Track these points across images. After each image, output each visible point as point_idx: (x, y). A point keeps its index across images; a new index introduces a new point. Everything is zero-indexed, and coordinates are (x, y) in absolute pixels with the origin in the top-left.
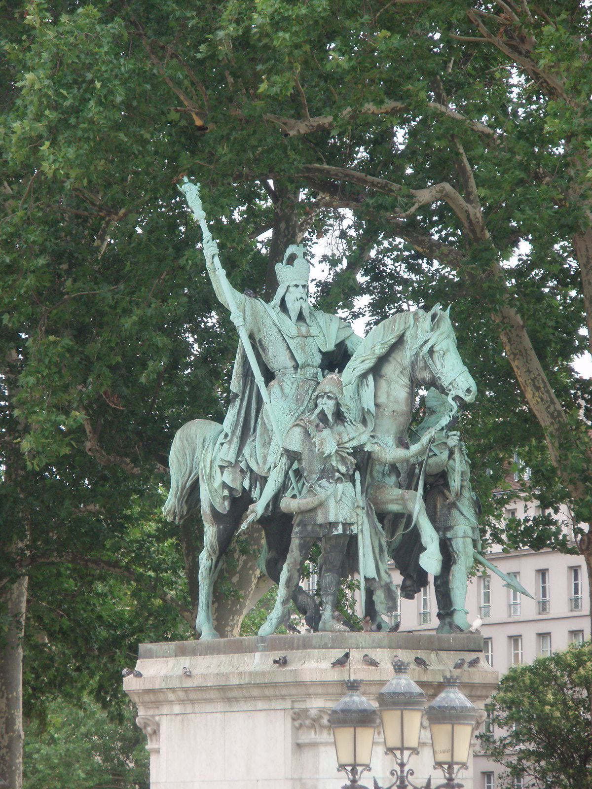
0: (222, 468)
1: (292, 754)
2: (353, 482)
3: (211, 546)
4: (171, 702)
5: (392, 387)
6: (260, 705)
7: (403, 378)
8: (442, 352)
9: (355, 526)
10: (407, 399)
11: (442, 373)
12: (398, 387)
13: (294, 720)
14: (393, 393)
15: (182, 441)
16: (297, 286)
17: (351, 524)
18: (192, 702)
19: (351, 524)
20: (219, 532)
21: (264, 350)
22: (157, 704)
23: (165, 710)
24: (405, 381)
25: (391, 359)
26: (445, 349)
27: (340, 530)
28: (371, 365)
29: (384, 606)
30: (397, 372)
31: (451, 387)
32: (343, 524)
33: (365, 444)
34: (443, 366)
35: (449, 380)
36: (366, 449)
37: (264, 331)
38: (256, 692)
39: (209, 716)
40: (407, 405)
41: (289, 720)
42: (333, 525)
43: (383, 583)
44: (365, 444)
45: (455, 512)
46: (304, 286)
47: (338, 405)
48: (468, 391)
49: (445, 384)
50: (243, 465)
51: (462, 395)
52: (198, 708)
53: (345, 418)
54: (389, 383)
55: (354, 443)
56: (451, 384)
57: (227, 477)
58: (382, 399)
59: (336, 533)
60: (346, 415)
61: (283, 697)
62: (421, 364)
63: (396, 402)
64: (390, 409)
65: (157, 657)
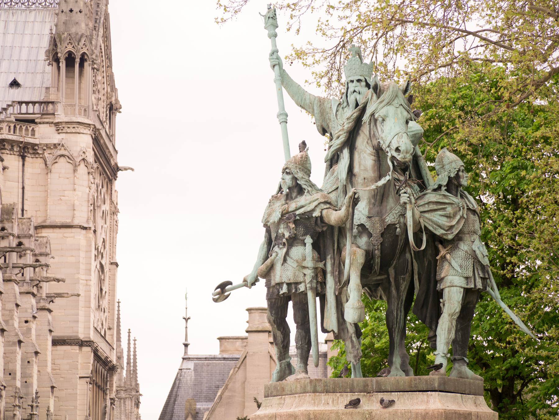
2: (305, 245)
5: (362, 157)
7: (368, 147)
8: (380, 119)
9: (303, 285)
10: (374, 166)
11: (382, 138)
12: (367, 156)
14: (363, 162)
16: (352, 81)
17: (297, 284)
19: (297, 284)
24: (370, 150)
25: (360, 132)
26: (381, 115)
27: (284, 289)
28: (343, 139)
29: (352, 355)
30: (365, 143)
31: (388, 149)
32: (289, 284)
33: (313, 210)
34: (383, 131)
35: (387, 144)
36: (314, 215)
37: (330, 126)
40: (374, 172)
42: (280, 284)
43: (350, 335)
44: (313, 210)
45: (446, 265)
46: (359, 81)
47: (295, 179)
48: (397, 150)
49: (384, 147)
51: (395, 154)
53: (305, 189)
54: (359, 154)
55: (301, 211)
56: (389, 146)
58: (356, 170)
59: (281, 292)
60: (304, 186)
62: (372, 133)
63: (366, 170)
64: (362, 177)
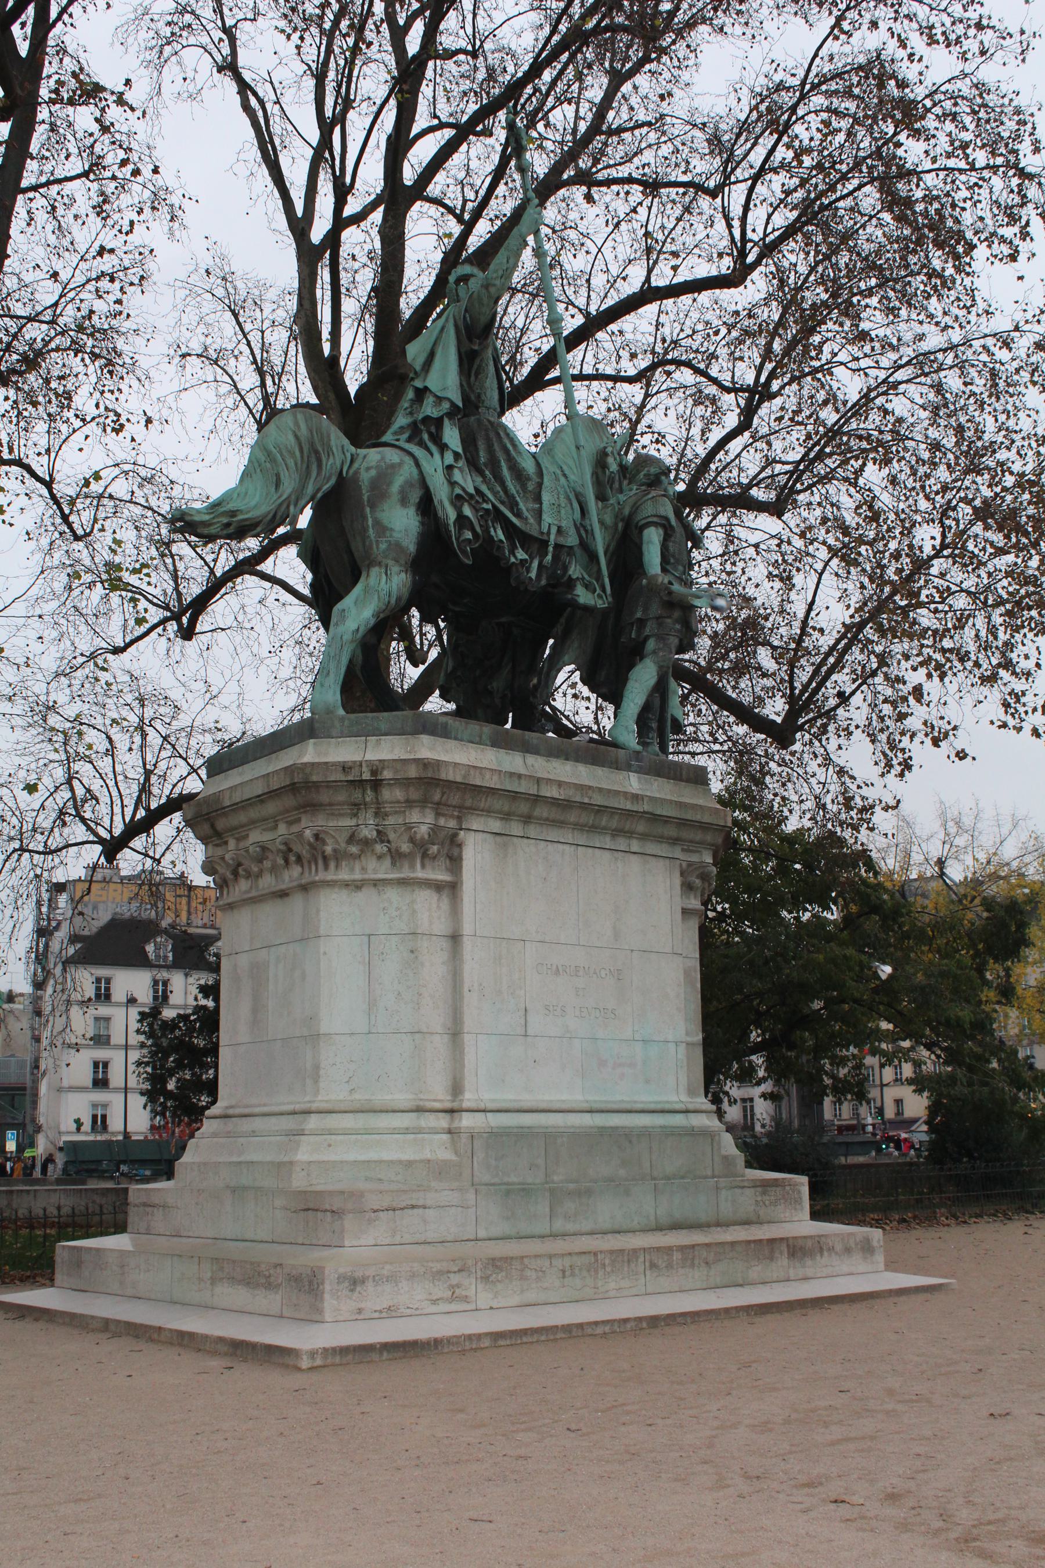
0: (458, 500)
1: (683, 919)
3: (399, 599)
4: (489, 812)
6: (635, 846)
13: (682, 874)
15: (311, 431)
18: (527, 819)
20: (414, 582)
21: (477, 374)
22: (462, 812)
23: (475, 823)
38: (641, 827)
39: (550, 846)
41: (678, 874)
50: (490, 506)
52: (532, 831)
57: (467, 511)
61: (674, 841)
65: (456, 739)
